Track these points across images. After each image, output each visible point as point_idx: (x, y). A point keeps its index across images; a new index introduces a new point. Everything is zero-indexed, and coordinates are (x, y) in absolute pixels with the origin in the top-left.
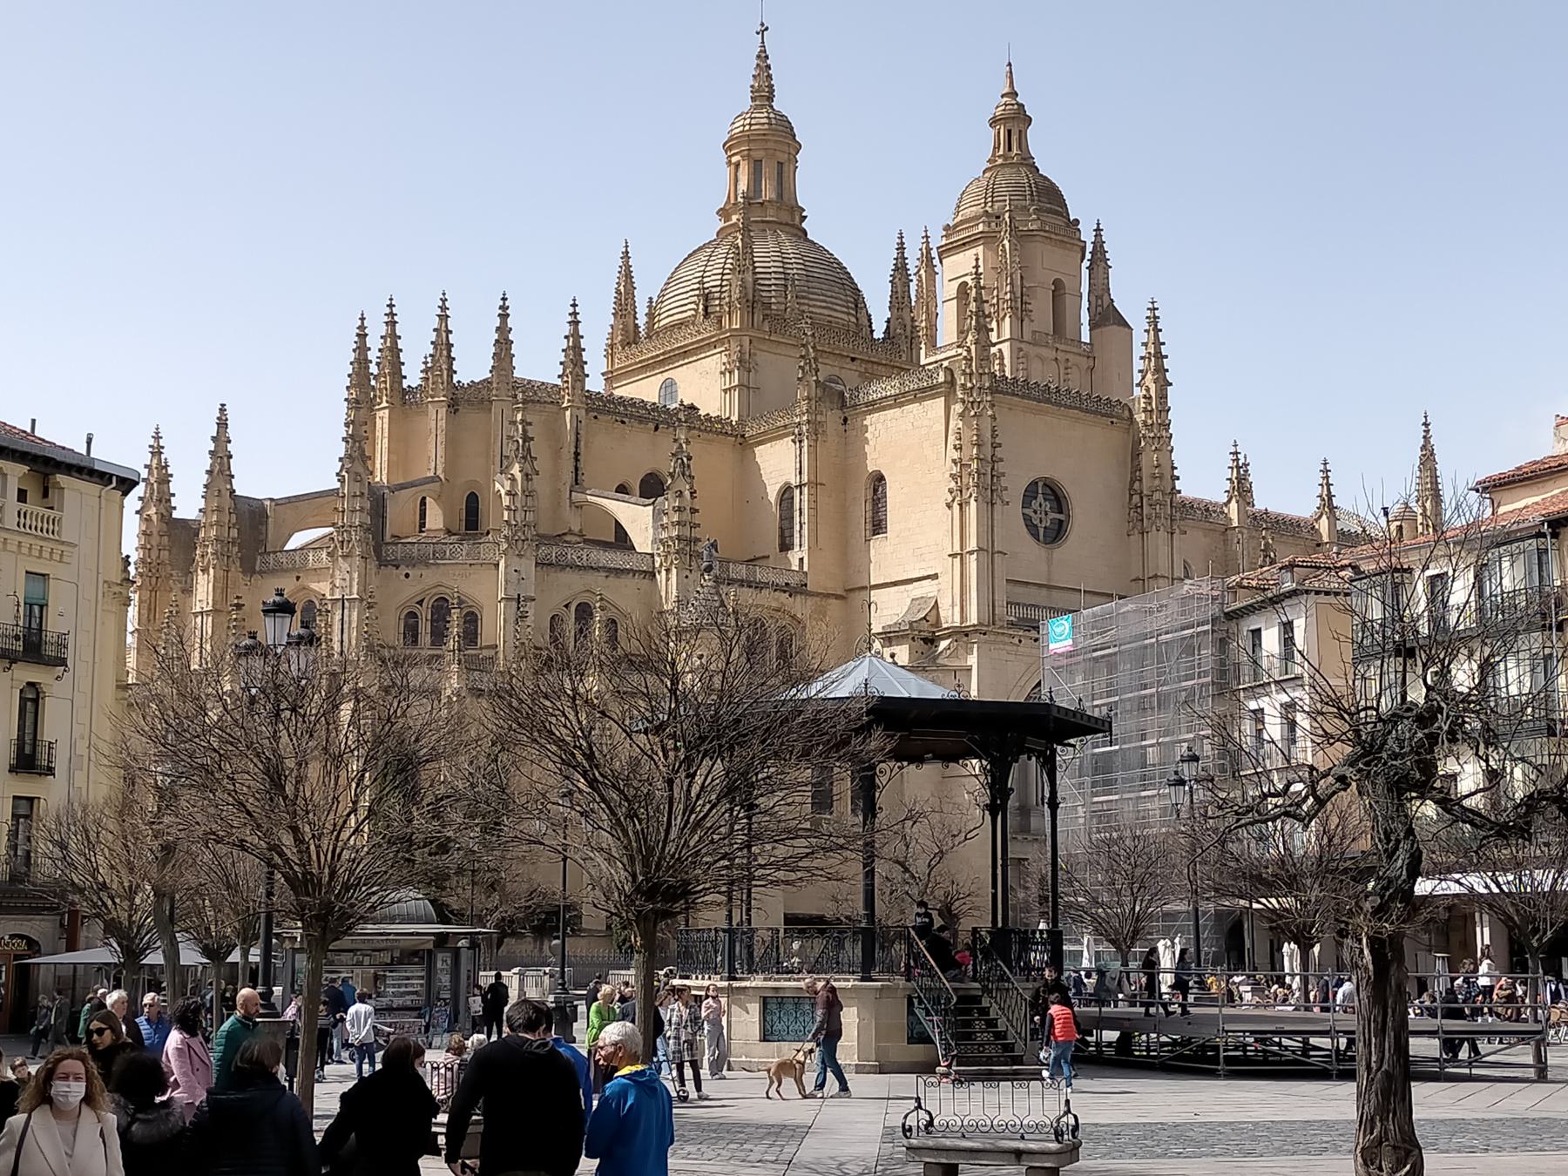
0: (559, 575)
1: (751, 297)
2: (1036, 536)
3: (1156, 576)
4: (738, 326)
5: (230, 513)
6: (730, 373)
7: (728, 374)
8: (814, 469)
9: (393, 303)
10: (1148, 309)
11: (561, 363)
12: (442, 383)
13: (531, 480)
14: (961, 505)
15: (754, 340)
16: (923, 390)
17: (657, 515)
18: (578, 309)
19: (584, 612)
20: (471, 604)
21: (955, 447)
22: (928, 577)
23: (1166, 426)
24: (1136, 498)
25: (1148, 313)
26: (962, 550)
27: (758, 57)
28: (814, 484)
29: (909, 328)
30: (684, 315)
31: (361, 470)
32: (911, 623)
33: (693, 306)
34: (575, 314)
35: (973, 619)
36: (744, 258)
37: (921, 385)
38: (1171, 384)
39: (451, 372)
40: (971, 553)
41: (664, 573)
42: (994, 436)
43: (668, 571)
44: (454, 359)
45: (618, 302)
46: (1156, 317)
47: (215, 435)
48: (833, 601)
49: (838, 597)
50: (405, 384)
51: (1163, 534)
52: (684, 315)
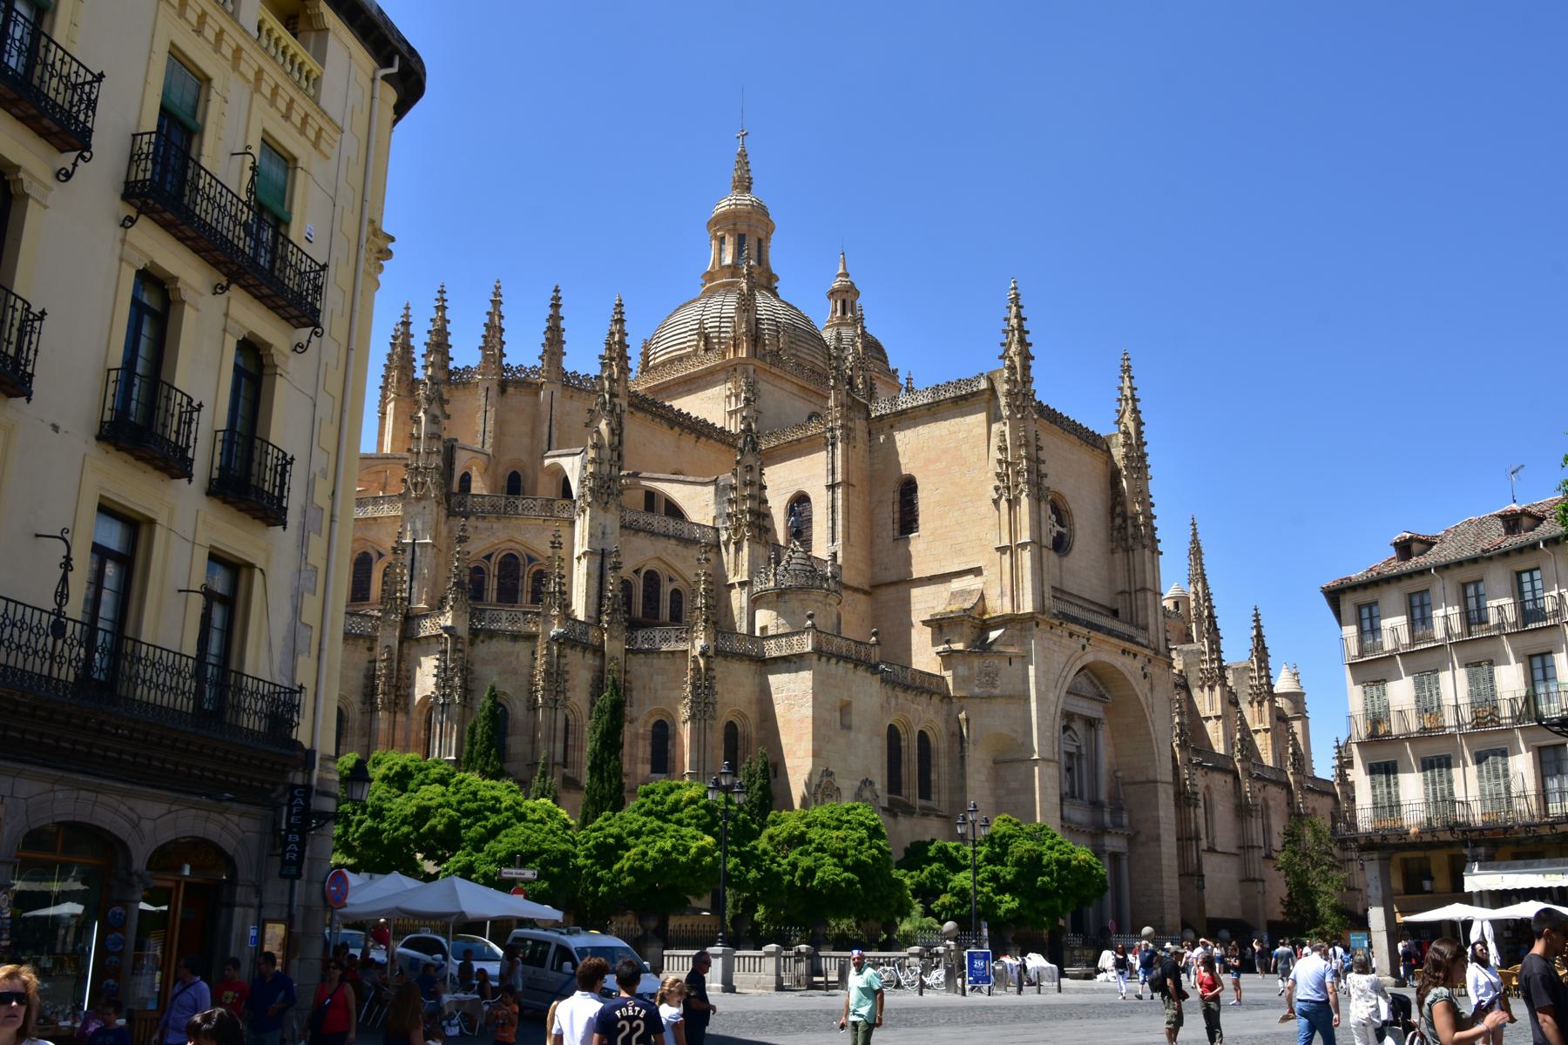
0: (632, 539)
3: (1144, 589)
4: (744, 356)
7: (733, 399)
8: (847, 470)
12: (494, 363)
14: (1009, 501)
15: (758, 370)
16: (963, 398)
17: (720, 491)
19: (652, 579)
21: (1000, 449)
23: (1143, 456)
24: (1118, 521)
28: (847, 484)
29: (869, 384)
30: (683, 352)
31: (438, 412)
32: (965, 610)
33: (695, 343)
35: (1027, 606)
36: (746, 305)
37: (958, 393)
38: (1144, 424)
40: (1023, 546)
41: (732, 548)
44: (504, 343)
46: (1128, 366)
49: (865, 592)
50: (452, 366)
51: (1147, 552)
52: (683, 352)
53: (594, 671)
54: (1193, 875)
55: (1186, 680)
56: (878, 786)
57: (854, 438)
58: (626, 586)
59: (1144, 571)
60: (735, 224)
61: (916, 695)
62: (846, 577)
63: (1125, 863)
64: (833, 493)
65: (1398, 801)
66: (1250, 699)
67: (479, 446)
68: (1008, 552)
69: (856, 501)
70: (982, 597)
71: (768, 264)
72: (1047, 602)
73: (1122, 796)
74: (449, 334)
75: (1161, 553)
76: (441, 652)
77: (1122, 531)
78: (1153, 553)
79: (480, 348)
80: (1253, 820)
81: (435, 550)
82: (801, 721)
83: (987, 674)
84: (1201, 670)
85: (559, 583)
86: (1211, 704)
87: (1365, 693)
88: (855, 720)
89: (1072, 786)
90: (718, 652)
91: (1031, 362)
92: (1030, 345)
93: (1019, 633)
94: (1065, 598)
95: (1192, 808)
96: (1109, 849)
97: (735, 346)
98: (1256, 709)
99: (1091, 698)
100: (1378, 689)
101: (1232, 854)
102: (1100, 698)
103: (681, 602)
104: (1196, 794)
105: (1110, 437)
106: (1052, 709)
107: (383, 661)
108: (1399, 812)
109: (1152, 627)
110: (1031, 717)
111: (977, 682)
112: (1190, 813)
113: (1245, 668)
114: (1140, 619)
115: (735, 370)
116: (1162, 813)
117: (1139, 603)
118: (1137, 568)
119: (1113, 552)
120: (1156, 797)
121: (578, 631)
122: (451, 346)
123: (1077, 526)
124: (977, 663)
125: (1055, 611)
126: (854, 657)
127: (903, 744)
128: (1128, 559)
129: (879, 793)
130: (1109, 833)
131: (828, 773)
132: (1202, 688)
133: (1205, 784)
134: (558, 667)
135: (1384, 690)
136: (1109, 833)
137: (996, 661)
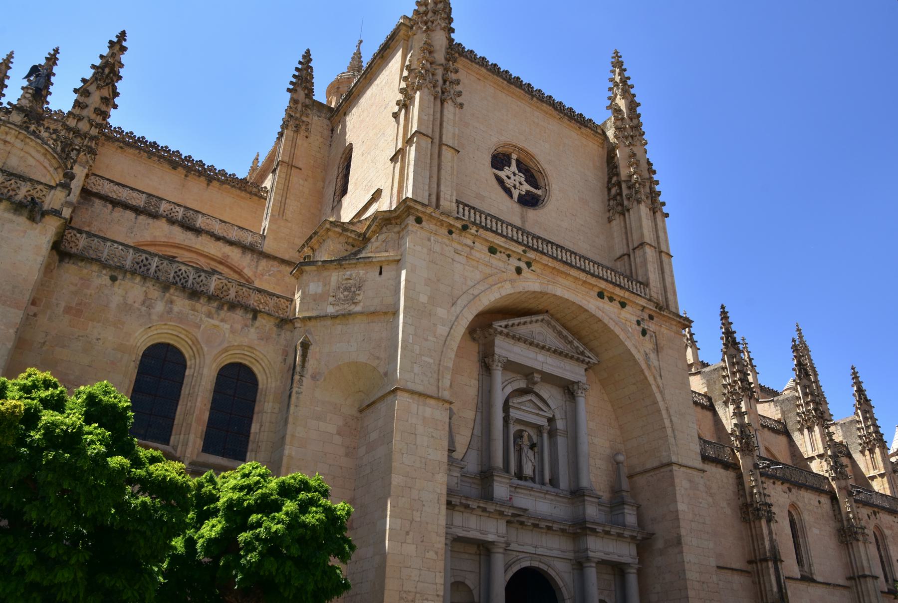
2: (511, 196)
3: (642, 245)
8: (292, 156)
23: (638, 127)
55: (785, 427)
59: (641, 226)
60: (338, 88)
62: (268, 246)
63: (632, 580)
66: (860, 448)
69: (301, 182)
75: (667, 215)
77: (618, 198)
78: (654, 211)
80: (860, 544)
83: (346, 289)
84: (798, 414)
86: (812, 445)
95: (764, 522)
98: (868, 457)
99: (560, 354)
101: (839, 586)
102: (578, 358)
104: (770, 505)
110: (398, 334)
111: (331, 299)
112: (761, 527)
113: (851, 422)
116: (682, 507)
117: (638, 260)
119: (610, 220)
120: (673, 484)
130: (594, 531)
132: (801, 431)
133: (788, 502)
136: (594, 531)
137: (362, 272)
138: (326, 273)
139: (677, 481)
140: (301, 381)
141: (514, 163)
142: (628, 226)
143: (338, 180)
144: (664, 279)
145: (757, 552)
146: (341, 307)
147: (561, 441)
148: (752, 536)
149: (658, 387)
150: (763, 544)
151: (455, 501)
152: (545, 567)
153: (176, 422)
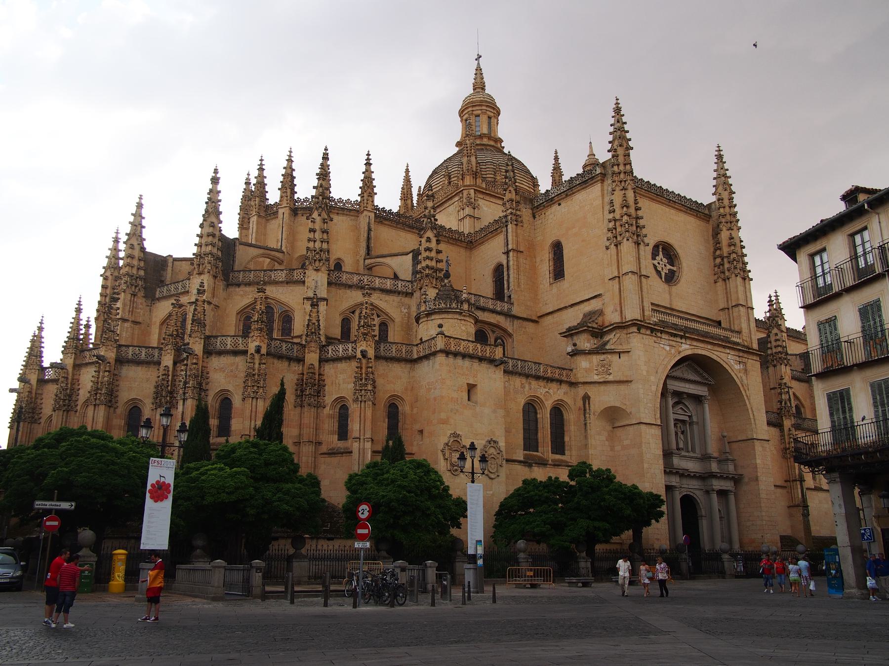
1: (474, 170)
2: (661, 278)
3: (737, 305)
5: (140, 260)
6: (463, 209)
8: (517, 243)
9: (263, 158)
10: (716, 151)
11: (360, 188)
12: (287, 197)
13: (327, 223)
14: (616, 246)
18: (370, 157)
20: (287, 309)
22: (595, 297)
24: (718, 260)
25: (717, 153)
26: (619, 273)
27: (476, 70)
31: (214, 220)
34: (368, 159)
38: (734, 193)
39: (293, 193)
42: (636, 204)
43: (421, 289)
44: (295, 185)
45: (403, 193)
47: (134, 213)
48: (531, 324)
51: (739, 279)
52: (438, 189)
53: (298, 374)
54: (798, 506)
56: (502, 444)
57: (522, 222)
58: (346, 323)
61: (547, 382)
63: (732, 498)
64: (508, 257)
65: (852, 422)
67: (280, 247)
68: (617, 279)
69: (524, 261)
70: (601, 313)
71: (496, 132)
72: (647, 313)
73: (728, 450)
74: (266, 185)
75: (752, 280)
76: (184, 365)
78: (744, 279)
79: (279, 189)
81: (212, 306)
82: (435, 399)
83: (603, 366)
85: (260, 315)
87: (820, 330)
88: (479, 395)
89: (686, 443)
90: (378, 357)
91: (631, 151)
92: (630, 140)
93: (625, 336)
94: (674, 313)
96: (717, 488)
97: (462, 180)
100: (830, 326)
103: (387, 331)
105: (711, 204)
106: (654, 388)
107: (163, 375)
108: (854, 434)
109: (745, 331)
111: (595, 372)
114: (736, 326)
115: (463, 194)
116: (758, 461)
117: (734, 314)
118: (731, 290)
119: (715, 282)
120: (754, 449)
121: (284, 348)
122: (267, 192)
123: (684, 265)
124: (596, 359)
125: (655, 320)
126: (480, 354)
127: (539, 416)
128: (726, 285)
129: (503, 449)
131: (455, 435)
134: (259, 370)
135: (835, 325)
137: (609, 356)
138: (590, 356)
139: (756, 448)
140: (590, 417)
141: (661, 253)
142: (728, 289)
143: (551, 262)
144: (749, 325)
145: (791, 476)
146: (602, 376)
147: (695, 427)
148: (788, 466)
149: (747, 396)
150: (795, 471)
151: (668, 470)
152: (692, 494)
153: (539, 441)
